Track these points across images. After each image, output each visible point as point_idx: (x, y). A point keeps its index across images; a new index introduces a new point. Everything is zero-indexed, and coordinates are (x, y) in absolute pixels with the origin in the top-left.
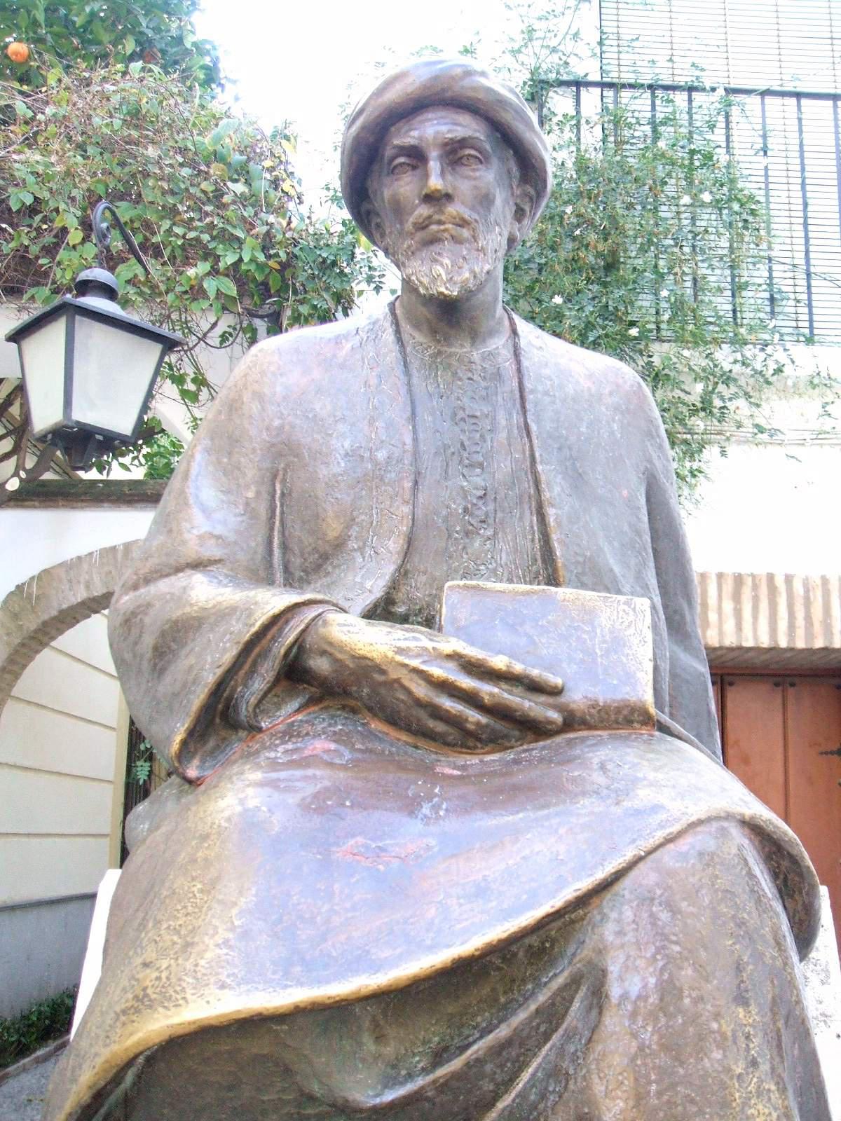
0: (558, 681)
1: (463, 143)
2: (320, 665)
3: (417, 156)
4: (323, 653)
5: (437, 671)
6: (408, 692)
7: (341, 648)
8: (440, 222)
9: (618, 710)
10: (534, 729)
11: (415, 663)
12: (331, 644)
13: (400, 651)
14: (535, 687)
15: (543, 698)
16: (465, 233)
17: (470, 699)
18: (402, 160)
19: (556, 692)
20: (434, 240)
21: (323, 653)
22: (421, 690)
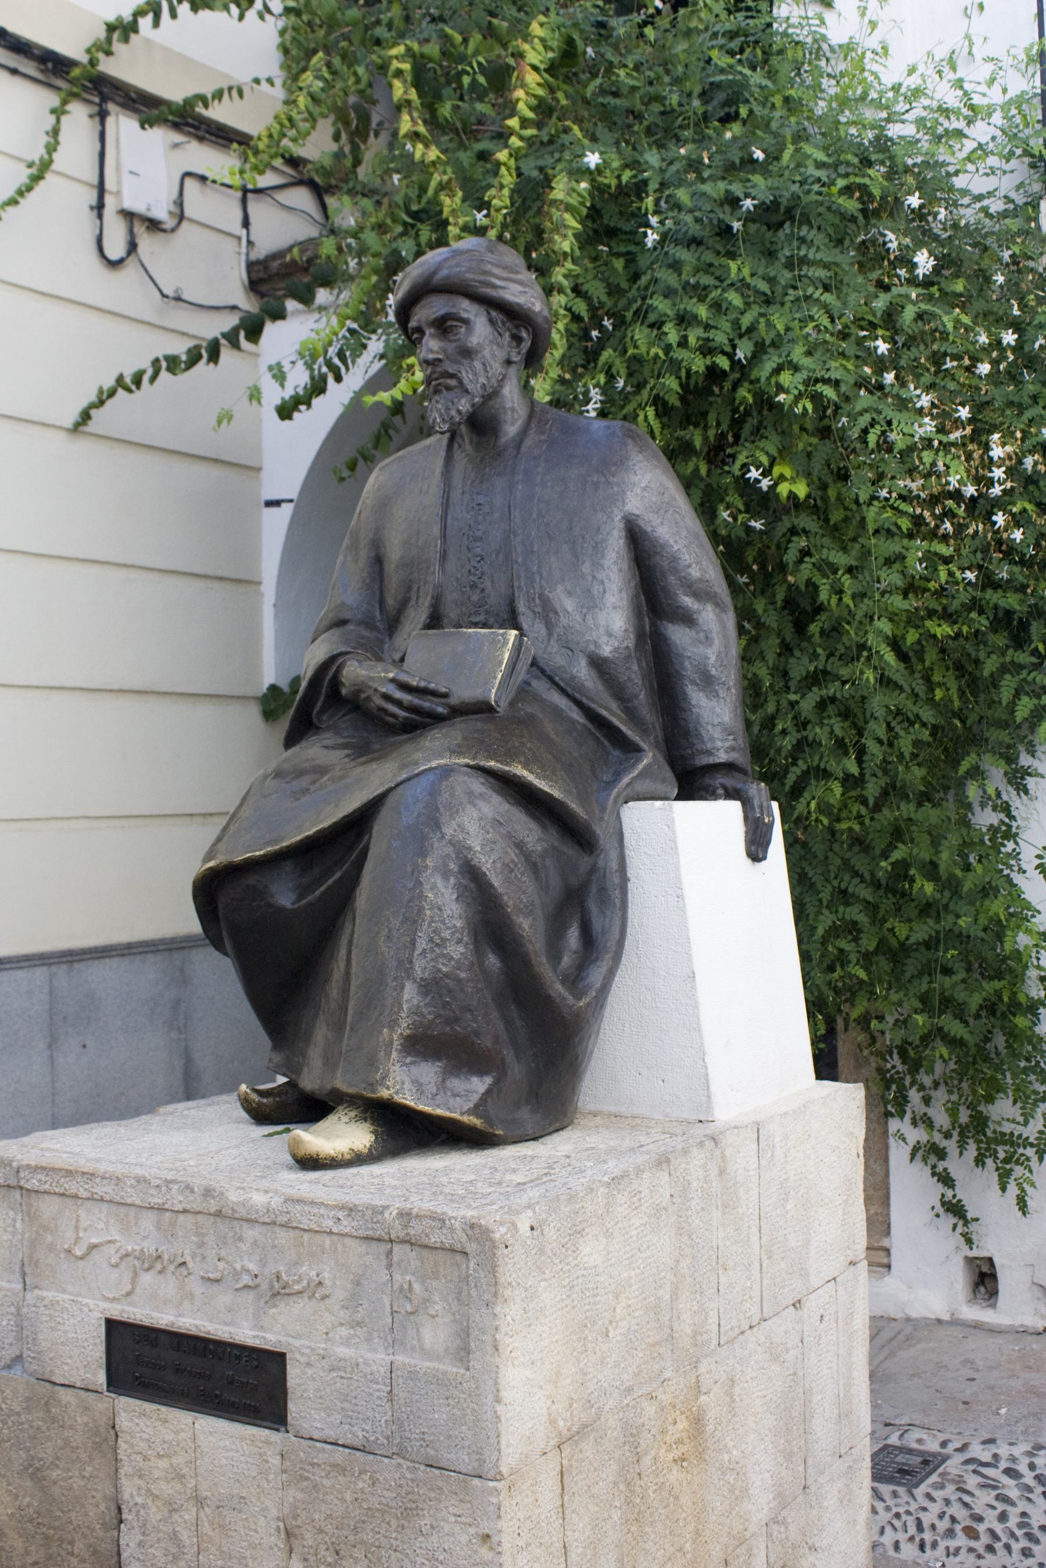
0: (444, 690)
9: (475, 704)
10: (437, 719)
13: (372, 678)
14: (434, 694)
15: (436, 700)
16: (453, 382)
17: (398, 703)
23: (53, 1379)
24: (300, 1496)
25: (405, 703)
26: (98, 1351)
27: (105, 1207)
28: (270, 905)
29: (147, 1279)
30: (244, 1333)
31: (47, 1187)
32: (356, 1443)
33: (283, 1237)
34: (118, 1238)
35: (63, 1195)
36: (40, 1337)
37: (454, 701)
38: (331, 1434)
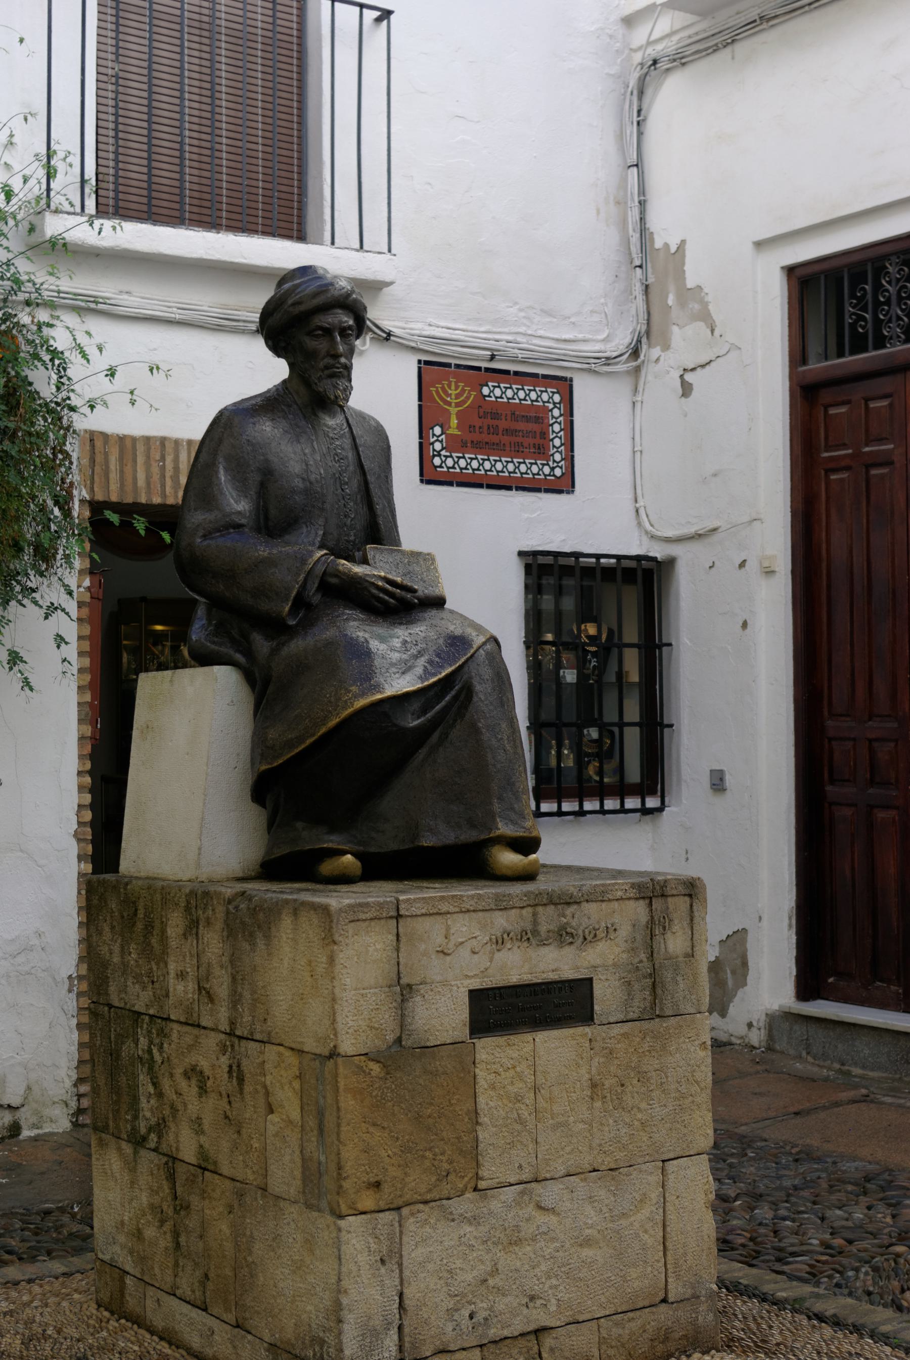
1: (350, 328)
2: (334, 580)
3: (328, 332)
4: (336, 576)
5: (380, 583)
6: (369, 592)
7: (344, 574)
8: (338, 368)
11: (373, 580)
12: (340, 572)
17: (391, 595)
18: (320, 332)
19: (415, 591)
20: (333, 376)
21: (336, 576)
22: (375, 591)
23: (428, 1044)
24: (602, 1060)
25: (398, 595)
26: (463, 1013)
27: (467, 916)
28: (395, 725)
29: (498, 955)
30: (569, 974)
31: (424, 911)
32: (635, 1016)
33: (591, 909)
34: (478, 933)
35: (437, 914)
36: (417, 1018)
37: (420, 593)
38: (621, 1017)
